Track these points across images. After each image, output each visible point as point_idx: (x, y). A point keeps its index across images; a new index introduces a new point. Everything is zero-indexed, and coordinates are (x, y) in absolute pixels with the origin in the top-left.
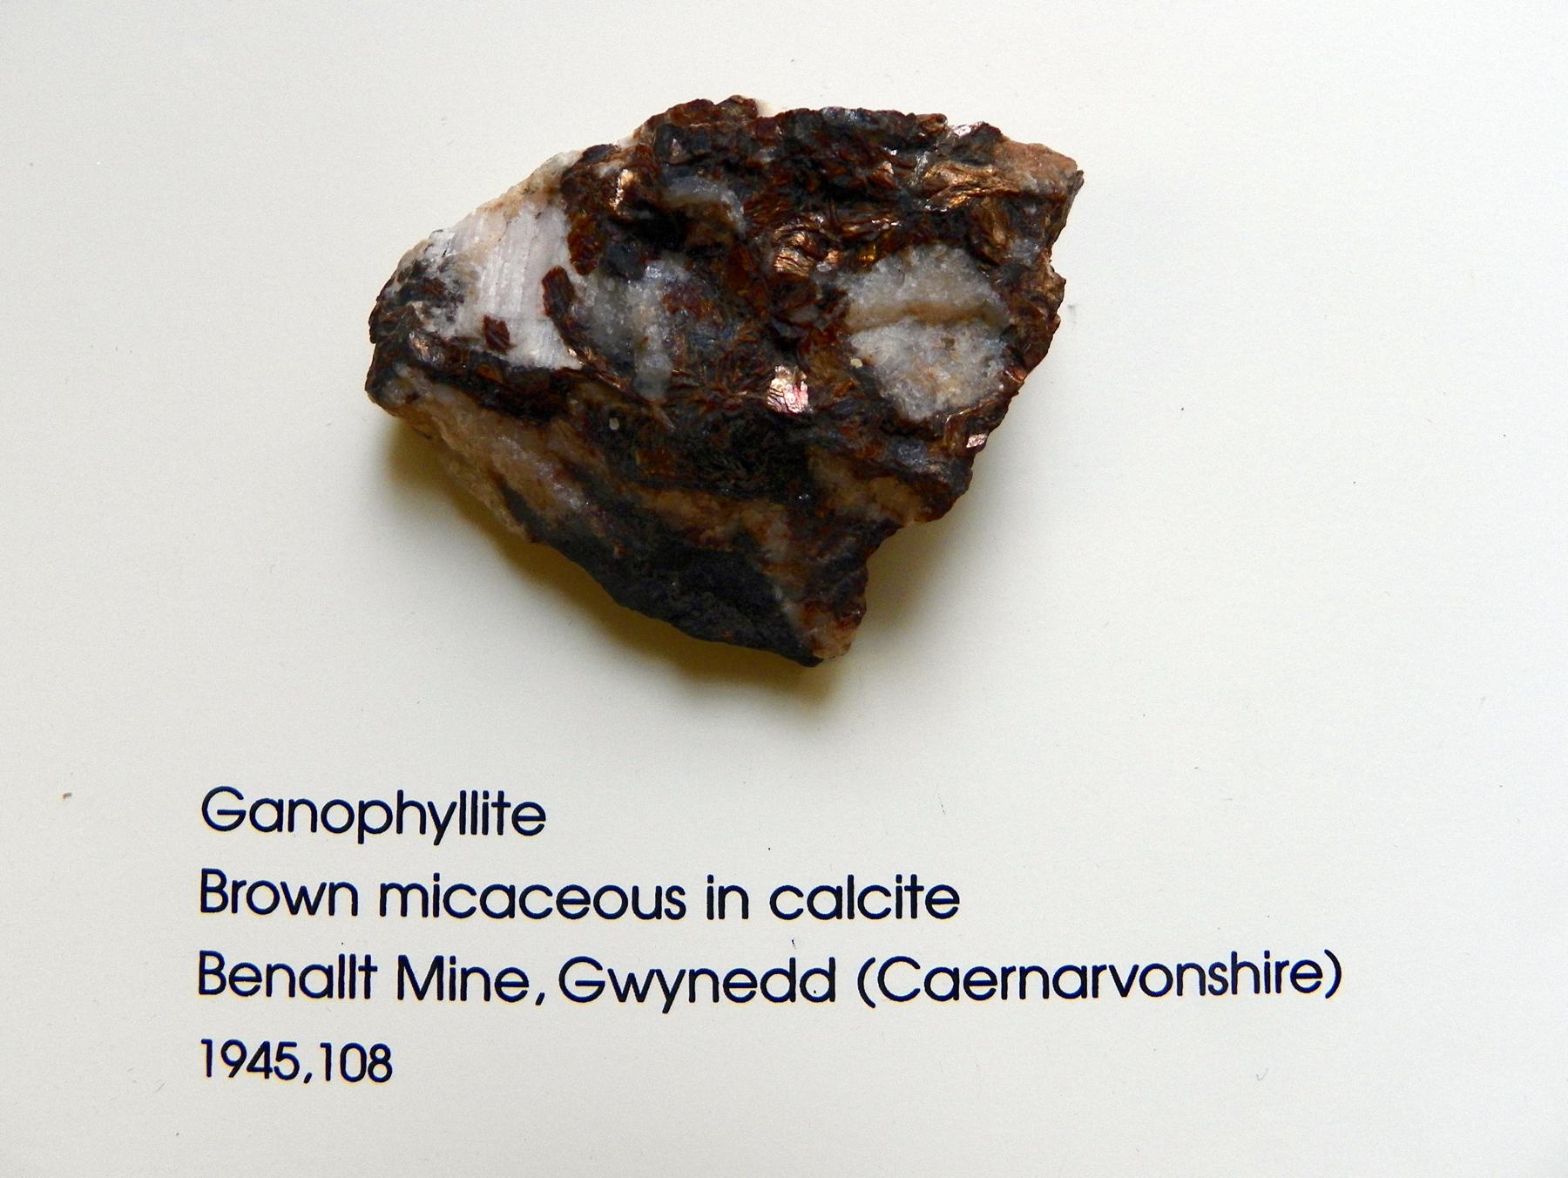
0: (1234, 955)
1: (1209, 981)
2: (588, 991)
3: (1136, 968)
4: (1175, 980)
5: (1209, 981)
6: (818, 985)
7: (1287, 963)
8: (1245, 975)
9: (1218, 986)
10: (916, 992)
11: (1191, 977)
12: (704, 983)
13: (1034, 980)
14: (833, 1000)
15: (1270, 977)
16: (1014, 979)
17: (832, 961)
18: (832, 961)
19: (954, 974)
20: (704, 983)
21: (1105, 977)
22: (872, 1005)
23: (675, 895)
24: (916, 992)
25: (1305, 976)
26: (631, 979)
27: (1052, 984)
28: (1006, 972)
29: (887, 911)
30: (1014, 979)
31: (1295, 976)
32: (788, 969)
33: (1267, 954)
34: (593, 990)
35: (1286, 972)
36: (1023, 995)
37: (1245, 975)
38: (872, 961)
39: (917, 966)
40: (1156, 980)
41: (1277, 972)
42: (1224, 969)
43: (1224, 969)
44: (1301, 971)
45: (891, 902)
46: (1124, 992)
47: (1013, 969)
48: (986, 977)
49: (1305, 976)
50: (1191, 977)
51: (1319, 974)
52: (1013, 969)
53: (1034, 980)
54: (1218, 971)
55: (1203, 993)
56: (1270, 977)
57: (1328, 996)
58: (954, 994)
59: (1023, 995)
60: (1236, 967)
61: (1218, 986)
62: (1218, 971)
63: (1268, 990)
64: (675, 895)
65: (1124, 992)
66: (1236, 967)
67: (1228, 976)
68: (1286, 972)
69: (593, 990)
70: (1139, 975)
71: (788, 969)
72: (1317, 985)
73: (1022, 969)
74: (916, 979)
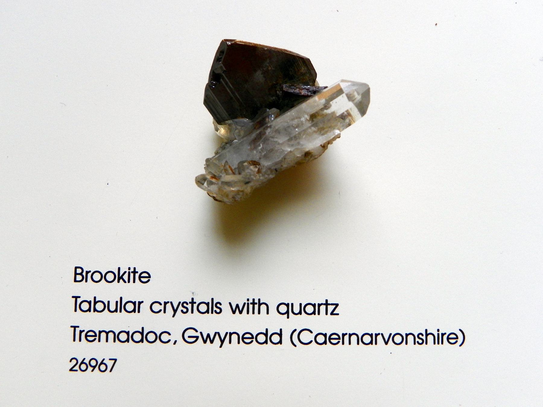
0: (426, 330)
1: (417, 339)
2: (193, 339)
3: (391, 334)
4: (405, 339)
5: (417, 339)
6: (276, 338)
7: (445, 334)
8: (430, 338)
9: (420, 341)
10: (311, 341)
11: (410, 338)
12: (234, 337)
13: (354, 338)
14: (281, 344)
15: (439, 339)
16: (346, 338)
17: (281, 330)
18: (281, 330)
19: (325, 335)
20: (234, 337)
21: (380, 338)
22: (295, 346)
23: (218, 305)
24: (311, 341)
25: (452, 338)
26: (208, 335)
27: (360, 340)
28: (344, 335)
29: (160, 310)
30: (346, 338)
31: (448, 339)
32: (265, 333)
33: (438, 330)
34: (194, 339)
35: (445, 337)
36: (350, 343)
37: (430, 338)
38: (295, 330)
39: (311, 332)
40: (398, 339)
41: (375, 338)
42: (423, 335)
43: (423, 335)
44: (451, 336)
45: (162, 307)
46: (386, 343)
47: (346, 334)
48: (336, 337)
49: (452, 338)
50: (410, 338)
51: (457, 338)
52: (346, 334)
53: (354, 338)
54: (420, 336)
55: (415, 344)
56: (439, 339)
57: (460, 346)
58: (325, 343)
59: (350, 344)
60: (427, 335)
61: (420, 341)
62: (420, 336)
63: (438, 343)
64: (218, 305)
65: (386, 343)
66: (427, 335)
67: (424, 338)
68: (445, 337)
69: (194, 339)
70: (392, 337)
71: (279, 333)
72: (456, 342)
73: (350, 334)
74: (311, 337)
